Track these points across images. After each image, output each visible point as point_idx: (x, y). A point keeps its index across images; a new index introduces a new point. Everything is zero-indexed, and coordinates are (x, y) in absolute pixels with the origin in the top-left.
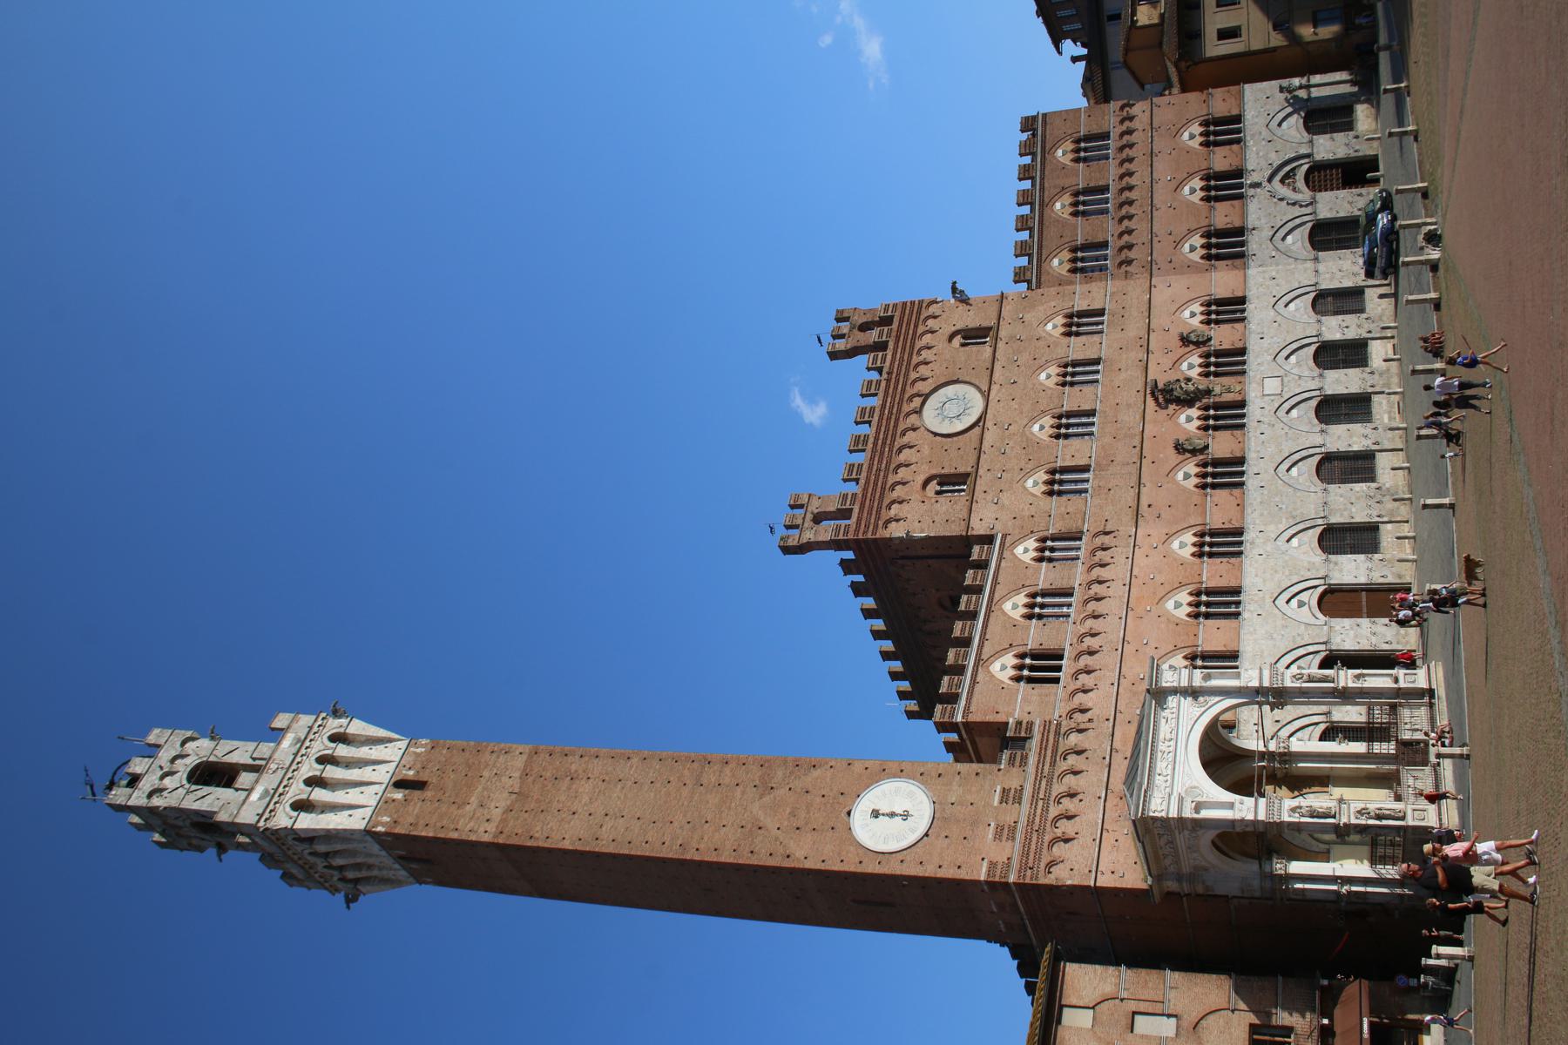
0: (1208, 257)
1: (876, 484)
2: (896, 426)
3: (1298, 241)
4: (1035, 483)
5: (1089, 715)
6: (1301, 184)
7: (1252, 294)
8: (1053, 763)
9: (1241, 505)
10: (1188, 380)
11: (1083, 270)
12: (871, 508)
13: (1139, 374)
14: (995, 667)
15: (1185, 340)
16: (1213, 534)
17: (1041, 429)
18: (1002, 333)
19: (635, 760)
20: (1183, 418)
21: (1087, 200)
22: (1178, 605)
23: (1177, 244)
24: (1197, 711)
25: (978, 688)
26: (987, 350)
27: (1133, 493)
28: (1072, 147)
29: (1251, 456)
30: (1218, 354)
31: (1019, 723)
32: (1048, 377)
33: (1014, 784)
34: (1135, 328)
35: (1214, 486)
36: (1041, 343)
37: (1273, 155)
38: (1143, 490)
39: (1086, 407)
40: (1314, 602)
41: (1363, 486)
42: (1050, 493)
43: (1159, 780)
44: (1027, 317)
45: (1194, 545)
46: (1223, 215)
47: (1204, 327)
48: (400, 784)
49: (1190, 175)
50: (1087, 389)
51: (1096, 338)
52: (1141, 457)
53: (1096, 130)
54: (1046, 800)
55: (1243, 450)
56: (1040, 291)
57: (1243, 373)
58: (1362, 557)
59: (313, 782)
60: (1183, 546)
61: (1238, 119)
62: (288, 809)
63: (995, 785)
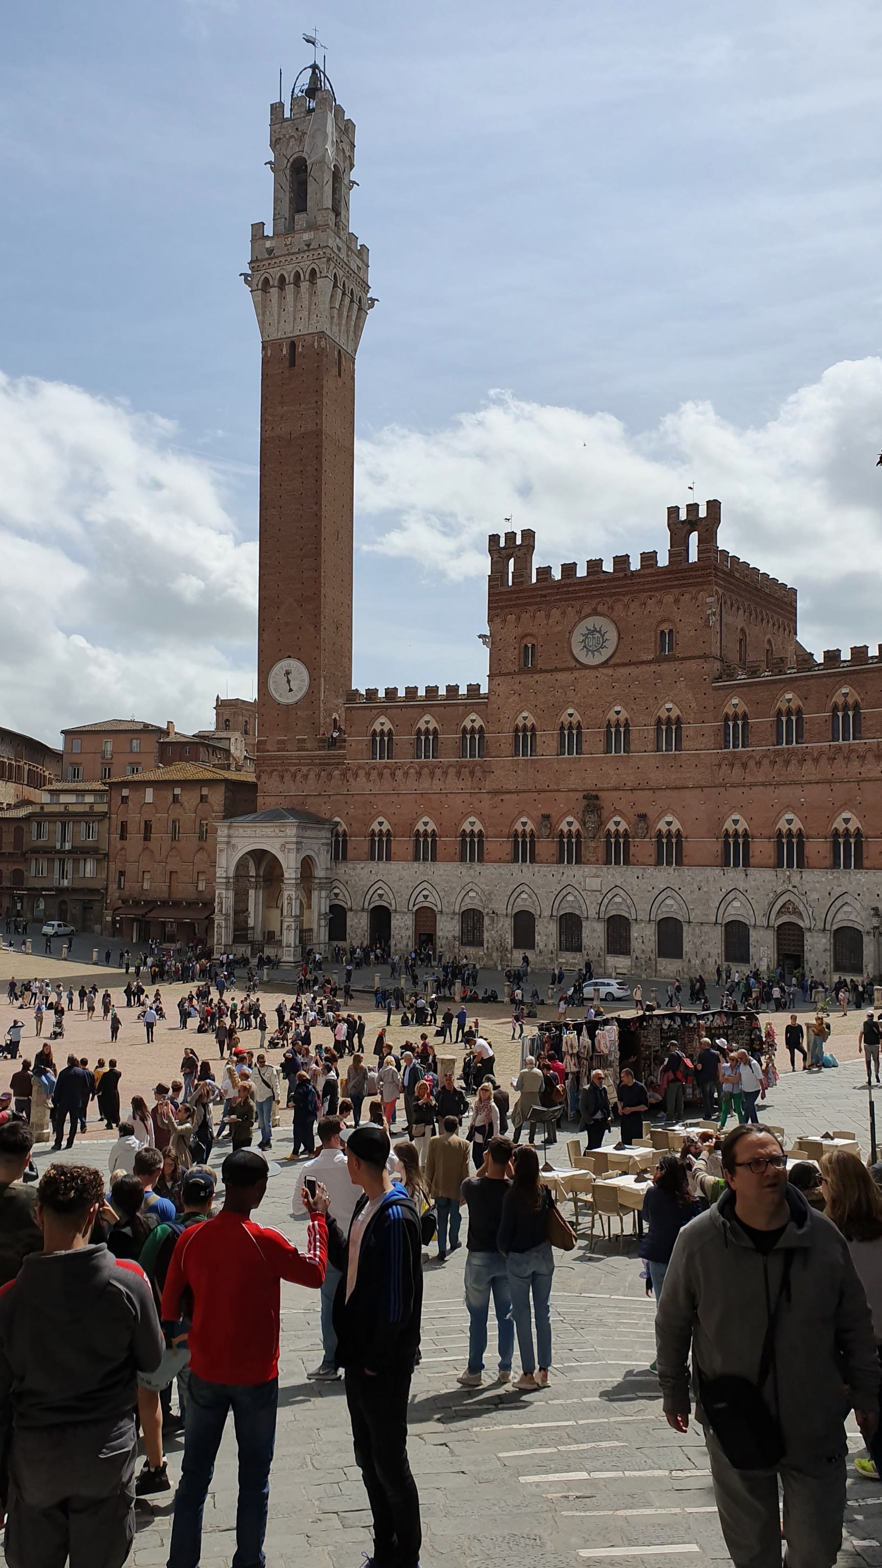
0: (727, 835)
1: (529, 597)
2: (579, 598)
3: (736, 910)
4: (526, 717)
5: (351, 780)
6: (785, 919)
7: (687, 872)
8: (320, 764)
9: (500, 861)
10: (602, 823)
11: (727, 726)
12: (511, 600)
13: (613, 783)
14: (383, 719)
15: (643, 817)
16: (481, 842)
17: (571, 714)
18: (665, 666)
19: (315, 508)
20: (570, 819)
21: (790, 725)
22: (426, 824)
23: (740, 809)
24: (278, 846)
25: (367, 712)
26: (651, 657)
27: (513, 787)
28: (850, 701)
29: (536, 867)
30: (626, 843)
31: (345, 741)
32: (618, 712)
33: (308, 745)
34: (656, 777)
35: (516, 842)
36: (651, 701)
37: (815, 896)
38: (514, 796)
39: (585, 747)
40: (426, 904)
41: (509, 940)
42: (517, 730)
43: (241, 830)
44: (681, 685)
45: (472, 831)
46: (762, 848)
47: (653, 833)
48: (293, 346)
49: (804, 820)
50: (601, 746)
51: (651, 747)
52: (539, 792)
53: (866, 723)
54: (299, 764)
55: (542, 862)
56: (711, 691)
57: (608, 862)
58: (457, 932)
59: (282, 279)
60: (472, 824)
61: (859, 866)
62: (262, 278)
63: (306, 734)
